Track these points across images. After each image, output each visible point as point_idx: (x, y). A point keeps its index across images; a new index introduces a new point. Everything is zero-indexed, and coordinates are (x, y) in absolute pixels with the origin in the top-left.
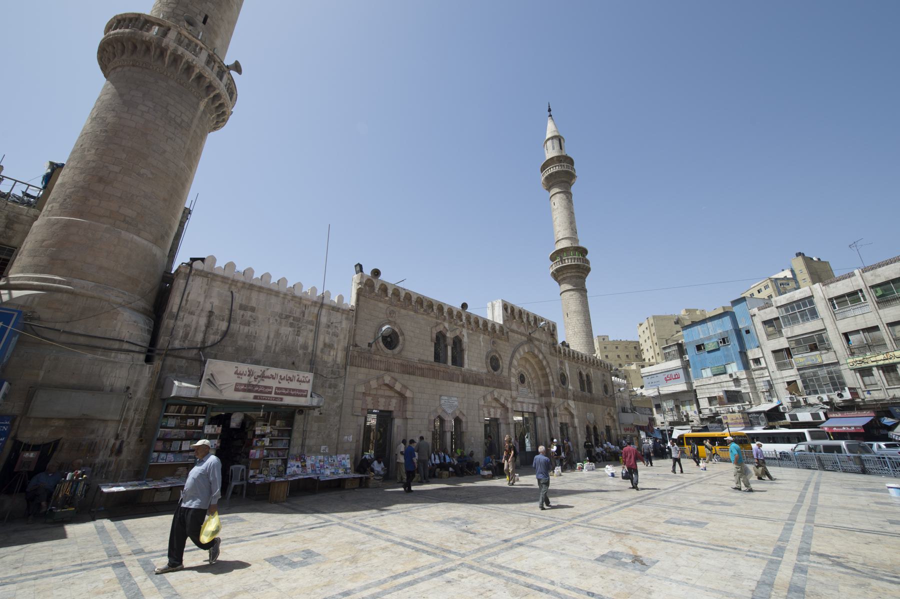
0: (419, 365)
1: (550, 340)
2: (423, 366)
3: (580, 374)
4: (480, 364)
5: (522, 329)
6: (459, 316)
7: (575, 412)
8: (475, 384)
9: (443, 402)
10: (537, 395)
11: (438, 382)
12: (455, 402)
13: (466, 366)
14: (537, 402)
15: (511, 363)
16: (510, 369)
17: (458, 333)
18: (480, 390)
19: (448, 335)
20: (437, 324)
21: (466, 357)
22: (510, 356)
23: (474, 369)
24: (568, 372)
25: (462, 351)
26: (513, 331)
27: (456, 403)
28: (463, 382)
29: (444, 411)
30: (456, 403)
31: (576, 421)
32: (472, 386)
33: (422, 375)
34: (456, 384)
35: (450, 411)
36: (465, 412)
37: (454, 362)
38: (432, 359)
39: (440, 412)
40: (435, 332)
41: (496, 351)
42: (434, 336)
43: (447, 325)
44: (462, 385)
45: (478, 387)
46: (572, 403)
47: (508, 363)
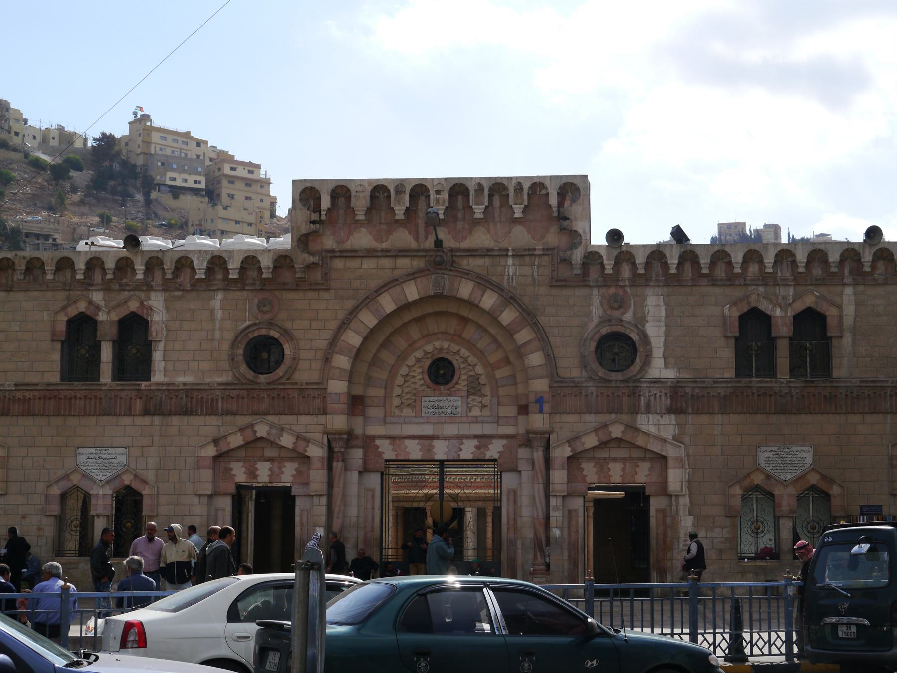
0: (19, 395)
1: (553, 238)
2: (28, 395)
3: (754, 322)
4: (205, 366)
5: (403, 238)
6: (124, 266)
7: (671, 452)
8: (187, 412)
9: (82, 459)
10: (512, 411)
11: (72, 421)
12: (119, 456)
13: (158, 377)
14: (509, 430)
15: (333, 343)
16: (327, 360)
17: (133, 306)
18: (208, 425)
19: (102, 317)
20: (71, 302)
21: (158, 355)
22: (334, 325)
23: (181, 379)
24: (655, 332)
25: (147, 348)
26: (353, 254)
27: (123, 459)
28: (146, 412)
29: (85, 476)
30: (123, 459)
31: (676, 478)
32: (175, 420)
33: (28, 413)
34: (126, 420)
35: (102, 476)
36: (151, 476)
37: (120, 373)
38: (57, 379)
39: (75, 479)
40: (63, 318)
41: (270, 324)
42: (62, 327)
43: (97, 297)
44: (147, 420)
45: (196, 420)
46: (657, 426)
47: (324, 344)
